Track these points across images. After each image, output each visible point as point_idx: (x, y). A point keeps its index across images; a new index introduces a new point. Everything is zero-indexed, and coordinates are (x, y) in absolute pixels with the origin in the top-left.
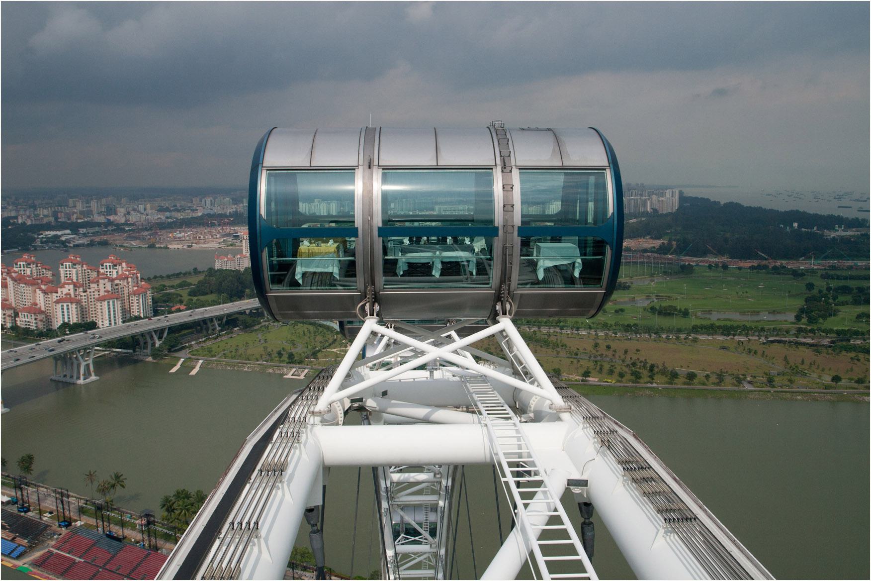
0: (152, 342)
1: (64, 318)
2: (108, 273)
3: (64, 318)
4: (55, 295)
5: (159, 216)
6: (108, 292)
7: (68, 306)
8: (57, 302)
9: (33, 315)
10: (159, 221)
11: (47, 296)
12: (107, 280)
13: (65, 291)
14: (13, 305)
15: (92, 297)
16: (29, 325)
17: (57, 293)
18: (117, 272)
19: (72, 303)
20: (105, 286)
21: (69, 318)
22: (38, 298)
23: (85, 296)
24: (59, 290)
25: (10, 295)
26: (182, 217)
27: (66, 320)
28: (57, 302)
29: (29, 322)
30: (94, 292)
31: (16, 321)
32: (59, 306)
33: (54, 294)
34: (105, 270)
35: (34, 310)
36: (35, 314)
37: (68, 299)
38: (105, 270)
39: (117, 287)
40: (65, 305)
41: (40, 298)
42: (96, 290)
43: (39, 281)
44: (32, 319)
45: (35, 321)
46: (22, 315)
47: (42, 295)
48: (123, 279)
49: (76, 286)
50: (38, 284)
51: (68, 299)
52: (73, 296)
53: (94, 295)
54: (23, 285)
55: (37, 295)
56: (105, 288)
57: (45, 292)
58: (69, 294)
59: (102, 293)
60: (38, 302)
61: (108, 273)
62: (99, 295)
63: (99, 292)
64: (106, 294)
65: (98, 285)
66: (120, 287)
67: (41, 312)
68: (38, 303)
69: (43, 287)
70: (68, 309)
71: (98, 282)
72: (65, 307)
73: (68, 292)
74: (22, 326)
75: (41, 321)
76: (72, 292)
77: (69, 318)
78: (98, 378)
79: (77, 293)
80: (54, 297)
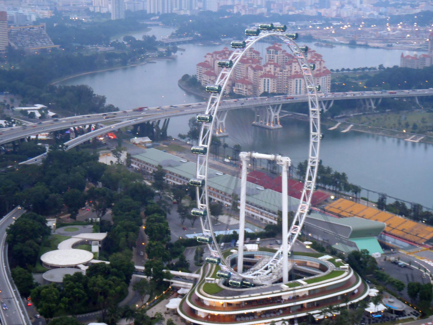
3: (265, 89)
5: (372, 12)
6: (297, 72)
8: (262, 77)
9: (245, 85)
10: (372, 17)
11: (255, 73)
13: (268, 69)
15: (286, 75)
16: (241, 93)
19: (271, 78)
20: (295, 68)
21: (268, 90)
23: (281, 74)
24: (264, 68)
26: (397, 14)
27: (266, 90)
28: (262, 77)
29: (241, 90)
30: (287, 72)
31: (232, 89)
32: (262, 80)
33: (260, 71)
36: (246, 84)
40: (267, 79)
42: (289, 71)
44: (243, 88)
46: (237, 85)
49: (276, 66)
50: (249, 63)
52: (273, 73)
53: (287, 74)
55: (249, 72)
56: (295, 69)
57: (254, 69)
59: (293, 73)
60: (249, 76)
62: (291, 74)
63: (291, 72)
64: (296, 74)
65: (291, 67)
68: (249, 77)
69: (254, 66)
70: (268, 82)
71: (291, 64)
72: (267, 81)
73: (270, 70)
74: (237, 93)
75: (249, 90)
77: (268, 90)
78: (280, 126)
79: (276, 72)
80: (260, 73)
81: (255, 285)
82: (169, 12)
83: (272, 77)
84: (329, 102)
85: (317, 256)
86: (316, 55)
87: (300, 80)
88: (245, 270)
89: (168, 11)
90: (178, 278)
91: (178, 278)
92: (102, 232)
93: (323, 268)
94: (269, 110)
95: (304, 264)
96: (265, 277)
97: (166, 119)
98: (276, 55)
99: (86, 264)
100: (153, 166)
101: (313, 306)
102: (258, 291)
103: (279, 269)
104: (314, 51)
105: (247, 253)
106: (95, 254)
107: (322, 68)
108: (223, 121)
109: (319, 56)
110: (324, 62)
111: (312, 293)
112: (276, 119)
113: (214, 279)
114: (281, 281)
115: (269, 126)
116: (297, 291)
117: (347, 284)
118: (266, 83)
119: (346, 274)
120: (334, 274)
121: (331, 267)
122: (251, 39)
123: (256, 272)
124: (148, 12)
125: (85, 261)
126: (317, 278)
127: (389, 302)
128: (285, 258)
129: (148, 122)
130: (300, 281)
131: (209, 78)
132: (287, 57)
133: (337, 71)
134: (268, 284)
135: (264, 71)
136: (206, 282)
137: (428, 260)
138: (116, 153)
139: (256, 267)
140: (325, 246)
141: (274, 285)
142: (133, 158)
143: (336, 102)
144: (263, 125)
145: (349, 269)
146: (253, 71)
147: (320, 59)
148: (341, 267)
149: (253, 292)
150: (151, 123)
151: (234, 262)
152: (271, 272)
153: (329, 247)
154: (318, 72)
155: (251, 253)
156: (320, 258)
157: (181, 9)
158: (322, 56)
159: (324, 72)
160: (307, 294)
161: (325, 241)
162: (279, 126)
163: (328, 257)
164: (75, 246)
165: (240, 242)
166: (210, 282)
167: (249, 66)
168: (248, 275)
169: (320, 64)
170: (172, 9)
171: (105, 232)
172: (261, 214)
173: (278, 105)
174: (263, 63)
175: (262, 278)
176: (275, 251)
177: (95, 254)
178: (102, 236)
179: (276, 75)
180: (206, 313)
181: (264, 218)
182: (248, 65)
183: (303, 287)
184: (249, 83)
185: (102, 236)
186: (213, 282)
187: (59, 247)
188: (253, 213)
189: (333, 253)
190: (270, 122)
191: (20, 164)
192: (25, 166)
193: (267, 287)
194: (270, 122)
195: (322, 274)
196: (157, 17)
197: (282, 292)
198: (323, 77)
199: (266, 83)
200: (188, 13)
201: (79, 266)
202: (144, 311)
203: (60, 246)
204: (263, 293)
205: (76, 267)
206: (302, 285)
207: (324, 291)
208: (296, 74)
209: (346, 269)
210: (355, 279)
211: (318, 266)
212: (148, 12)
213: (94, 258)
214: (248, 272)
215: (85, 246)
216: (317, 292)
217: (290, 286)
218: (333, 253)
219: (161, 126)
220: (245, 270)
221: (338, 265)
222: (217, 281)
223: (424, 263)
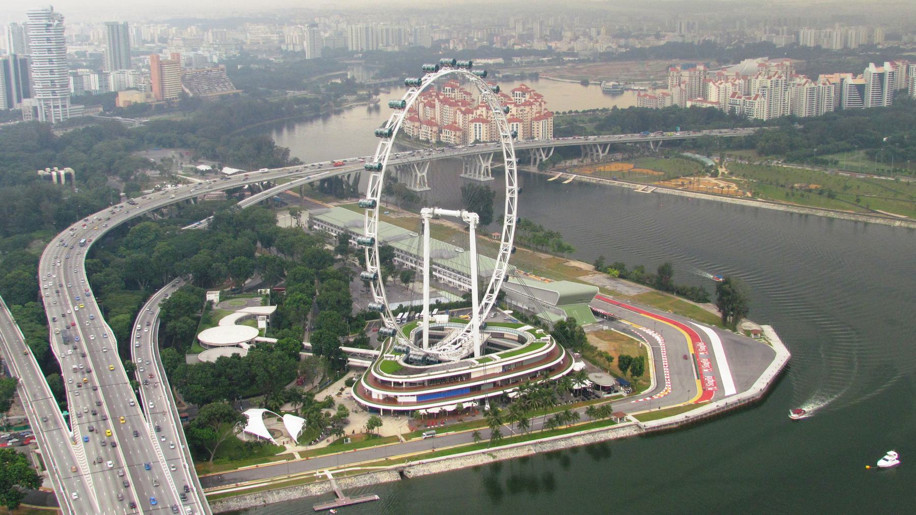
0: (541, 158)
1: (476, 136)
2: (518, 101)
4: (471, 115)
5: (610, 44)
7: (480, 125)
8: (472, 121)
10: (609, 50)
12: (513, 105)
13: (479, 112)
14: (439, 124)
17: (473, 114)
18: (525, 100)
19: (483, 122)
21: (480, 136)
22: (457, 118)
24: (475, 112)
25: (436, 114)
26: (639, 46)
27: (478, 138)
28: (472, 121)
31: (440, 136)
32: (473, 125)
34: (516, 98)
35: (453, 127)
37: (479, 120)
38: (516, 98)
39: (522, 113)
41: (460, 118)
43: (460, 104)
45: (453, 137)
47: (461, 115)
48: (527, 105)
50: (458, 105)
51: (479, 120)
52: (485, 117)
54: (447, 106)
55: (457, 115)
57: (464, 113)
58: (482, 115)
61: (518, 101)
64: (512, 117)
66: (525, 112)
67: (459, 129)
69: (463, 109)
70: (480, 128)
72: (478, 126)
74: (444, 141)
75: (459, 137)
76: (484, 114)
77: (480, 136)
80: (470, 117)
81: (440, 362)
82: (375, 49)
83: (485, 121)
84: (549, 149)
85: (517, 326)
86: (536, 95)
87: (517, 125)
88: (431, 344)
89: (373, 48)
90: (354, 355)
91: (354, 355)
92: (272, 304)
93: (522, 340)
94: (480, 161)
95: (501, 336)
96: (453, 352)
97: (357, 173)
98: (453, 94)
99: (249, 343)
100: (338, 228)
101: (506, 383)
102: (443, 368)
103: (470, 342)
104: (534, 91)
105: (432, 325)
106: (261, 330)
107: (543, 110)
108: (425, 174)
109: (539, 96)
110: (545, 103)
111: (506, 369)
112: (487, 170)
113: (394, 355)
114: (472, 355)
115: (479, 179)
116: (487, 367)
117: (550, 356)
118: (478, 129)
119: (547, 345)
120: (533, 346)
121: (531, 338)
122: (430, 76)
123: (443, 347)
124: (350, 49)
125: (249, 338)
126: (513, 352)
127: (596, 377)
128: (476, 331)
129: (336, 177)
130: (493, 355)
131: (412, 124)
132: (502, 98)
133: (564, 113)
134: (457, 360)
135: (475, 114)
136: (385, 359)
137: (647, 328)
138: (295, 214)
139: (445, 341)
140: (528, 315)
141: (462, 361)
142: (315, 219)
143: (558, 149)
144: (472, 177)
145: (551, 338)
146: (462, 115)
147: (540, 100)
148: (542, 338)
149: (437, 369)
150: (340, 177)
151: (419, 335)
152: (461, 346)
153: (534, 316)
154: (538, 115)
155: (440, 325)
156: (519, 329)
157: (387, 45)
158: (542, 96)
159: (545, 115)
160: (501, 370)
161: (530, 309)
162: (490, 178)
163: (529, 327)
164: (239, 322)
165: (425, 312)
166: (389, 359)
167: (458, 109)
168: (434, 350)
169: (540, 105)
170: (377, 45)
171: (275, 305)
172: (459, 280)
173: (490, 154)
174: (475, 104)
175: (449, 353)
176: (467, 322)
177: (261, 330)
178: (270, 309)
179: (489, 119)
180: (383, 395)
181: (462, 284)
182: (457, 108)
183: (496, 362)
184: (458, 129)
185: (270, 309)
186: (393, 359)
187: (220, 324)
188: (450, 280)
189: (537, 323)
190: (479, 173)
191: (183, 229)
192: (188, 230)
193: (454, 363)
194: (479, 173)
195: (521, 347)
196: (361, 55)
197: (471, 368)
198: (544, 121)
199: (478, 129)
200: (397, 49)
201: (241, 344)
202: (313, 395)
203: (221, 322)
204: (450, 370)
205: (238, 346)
206: (496, 360)
207: (520, 366)
208: (512, 117)
209: (548, 340)
210: (559, 350)
211: (517, 339)
212: (350, 49)
213: (260, 335)
214: (435, 347)
215: (249, 321)
216: (513, 367)
217: (480, 361)
218: (537, 323)
219: (351, 182)
220: (431, 344)
221: (538, 336)
222: (398, 357)
223: (641, 332)
